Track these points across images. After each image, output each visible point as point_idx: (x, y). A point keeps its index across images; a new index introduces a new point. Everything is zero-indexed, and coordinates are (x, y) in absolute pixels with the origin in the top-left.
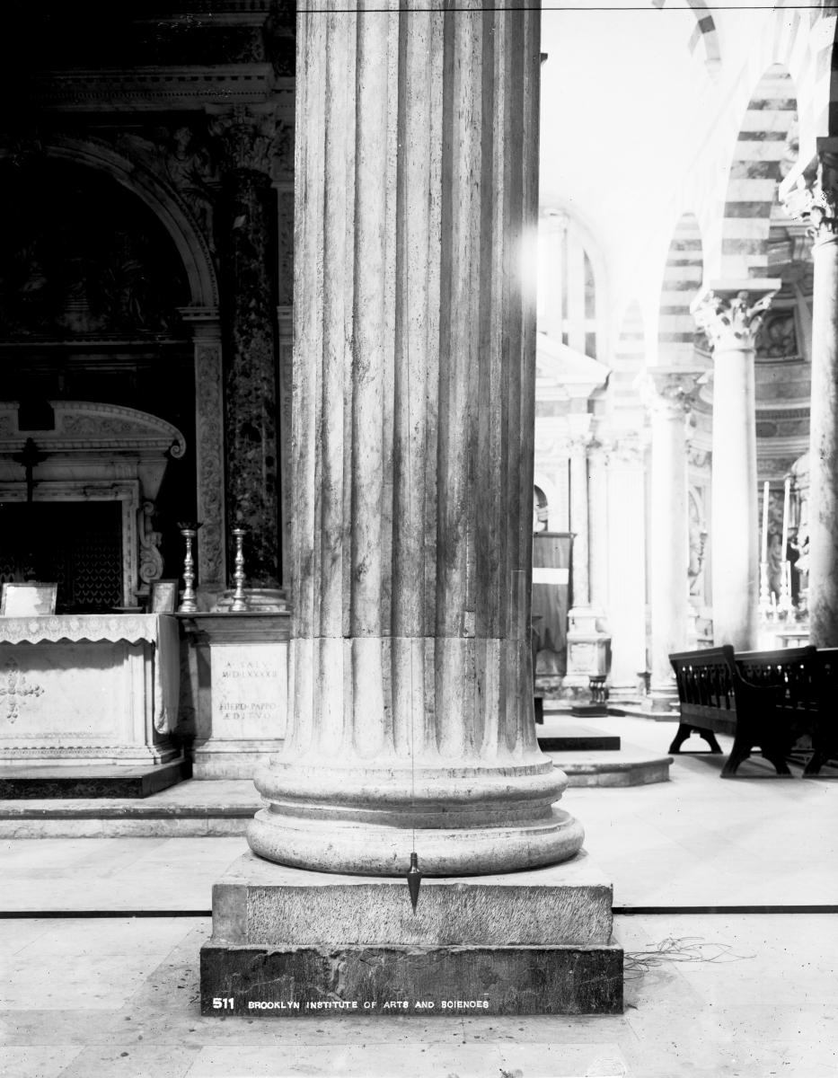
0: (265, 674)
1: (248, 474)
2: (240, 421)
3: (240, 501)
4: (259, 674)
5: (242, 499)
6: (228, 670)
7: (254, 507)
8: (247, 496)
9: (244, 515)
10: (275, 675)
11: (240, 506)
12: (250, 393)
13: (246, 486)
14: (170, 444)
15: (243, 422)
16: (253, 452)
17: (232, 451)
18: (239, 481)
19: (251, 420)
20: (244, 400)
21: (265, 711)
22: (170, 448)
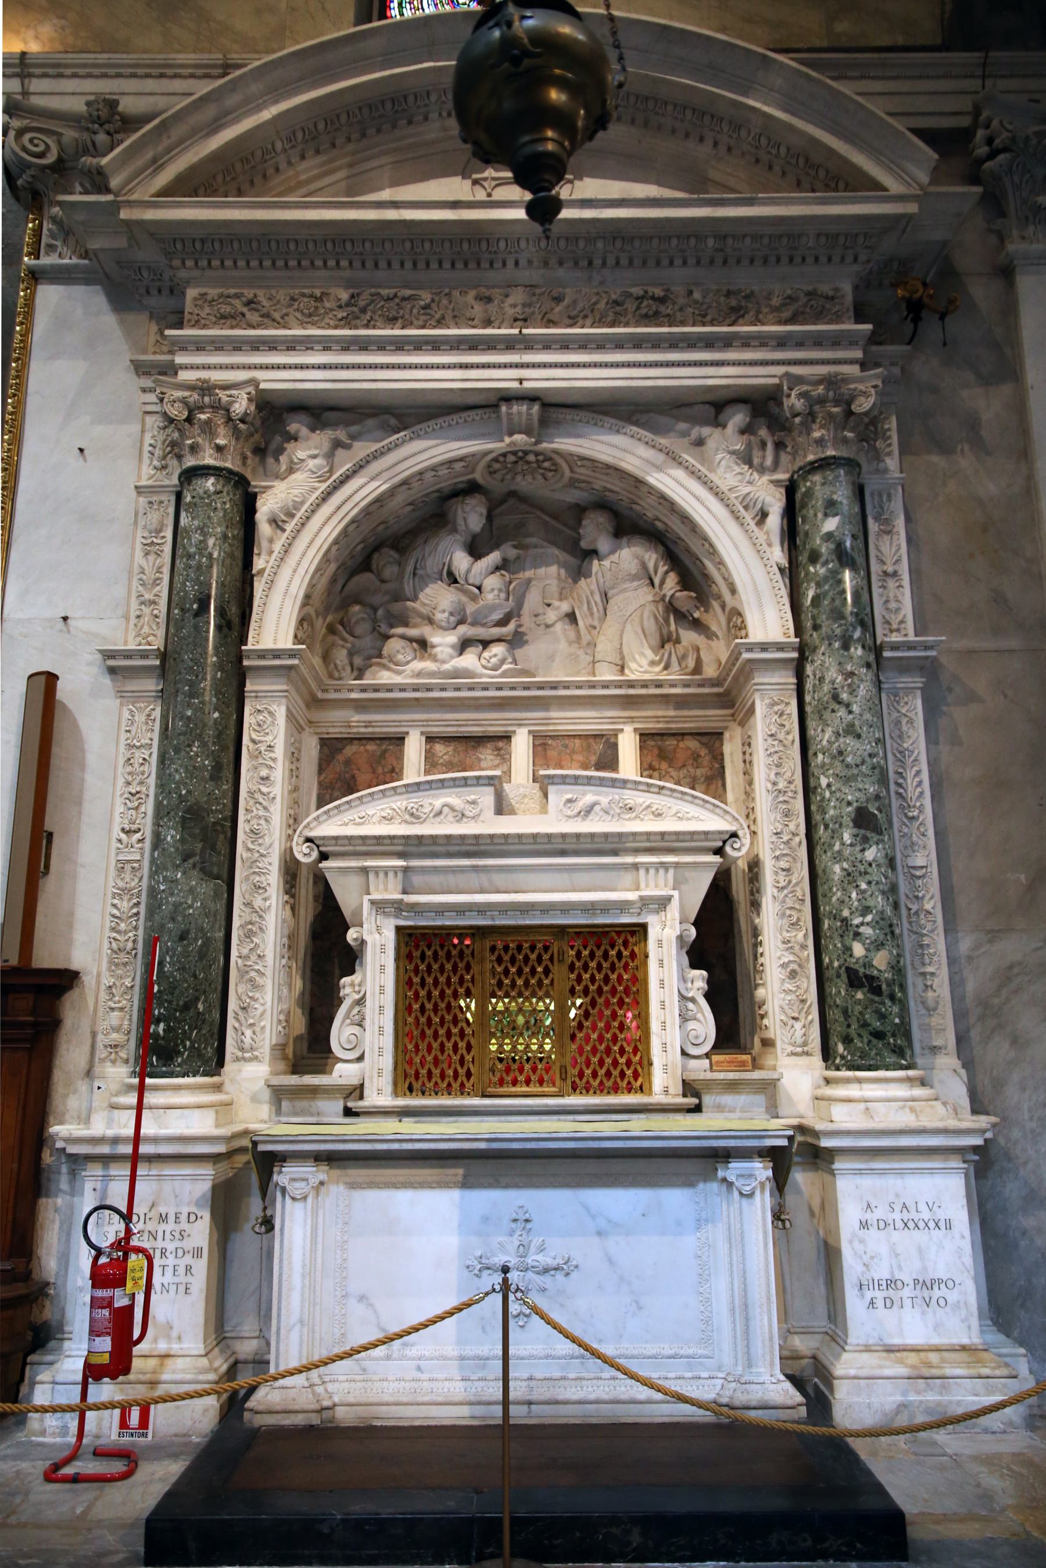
0: (932, 1225)
1: (869, 883)
2: (849, 804)
3: (857, 926)
4: (921, 1225)
5: (862, 924)
6: (872, 1217)
7: (882, 937)
8: (869, 918)
9: (867, 950)
10: (949, 1225)
11: (857, 934)
12: (863, 762)
13: (868, 904)
14: (727, 836)
15: (855, 805)
16: (874, 849)
17: (837, 847)
18: (854, 895)
19: (868, 800)
20: (855, 771)
21: (936, 1293)
22: (724, 842)
